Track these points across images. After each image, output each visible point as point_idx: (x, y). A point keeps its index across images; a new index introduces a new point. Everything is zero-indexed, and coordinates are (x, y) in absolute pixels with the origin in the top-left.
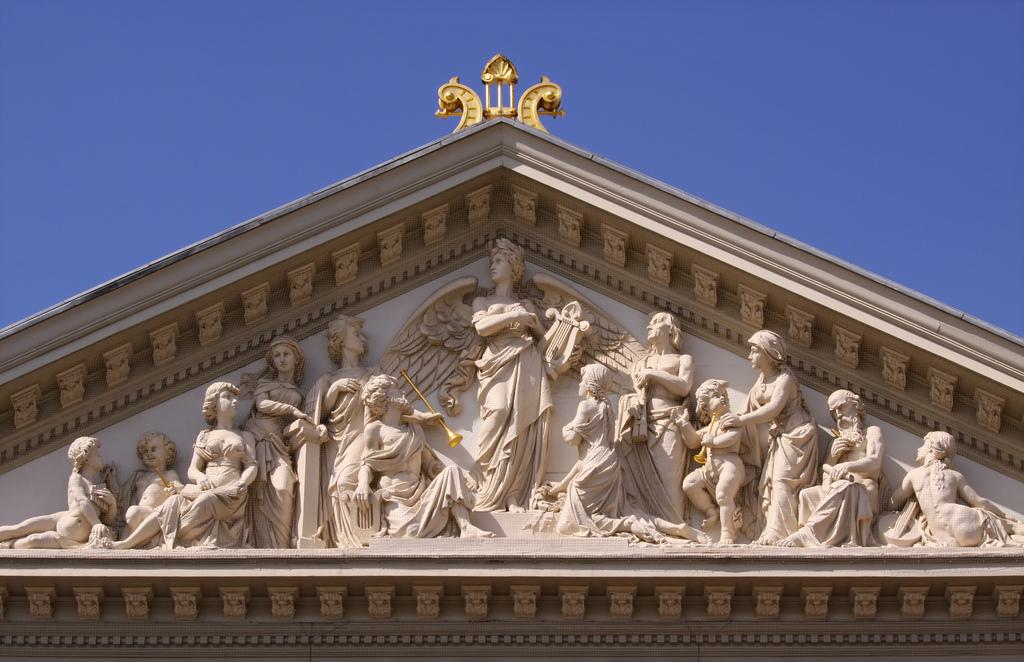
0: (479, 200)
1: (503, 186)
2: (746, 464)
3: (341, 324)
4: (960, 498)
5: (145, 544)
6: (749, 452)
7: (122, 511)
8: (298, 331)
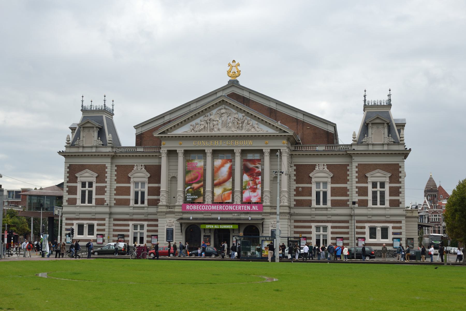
4: (258, 128)
5: (196, 132)
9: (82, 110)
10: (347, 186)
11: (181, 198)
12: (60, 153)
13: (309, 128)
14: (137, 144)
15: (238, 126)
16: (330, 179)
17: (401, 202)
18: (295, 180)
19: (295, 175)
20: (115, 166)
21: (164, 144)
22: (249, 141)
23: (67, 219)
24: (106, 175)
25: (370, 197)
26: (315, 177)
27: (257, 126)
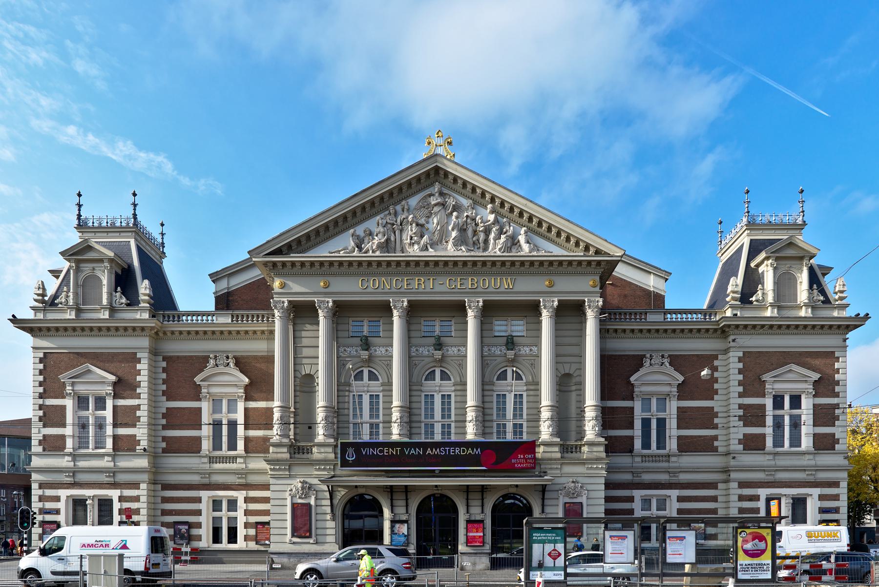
0: (432, 173)
1: (437, 169)
2: (486, 235)
3: (404, 202)
6: (487, 231)
7: (361, 245)
8: (395, 204)
10: (715, 404)
14: (217, 308)
16: (676, 389)
17: (838, 440)
20: (161, 358)
23: (42, 486)
24: (139, 378)
25: (769, 430)
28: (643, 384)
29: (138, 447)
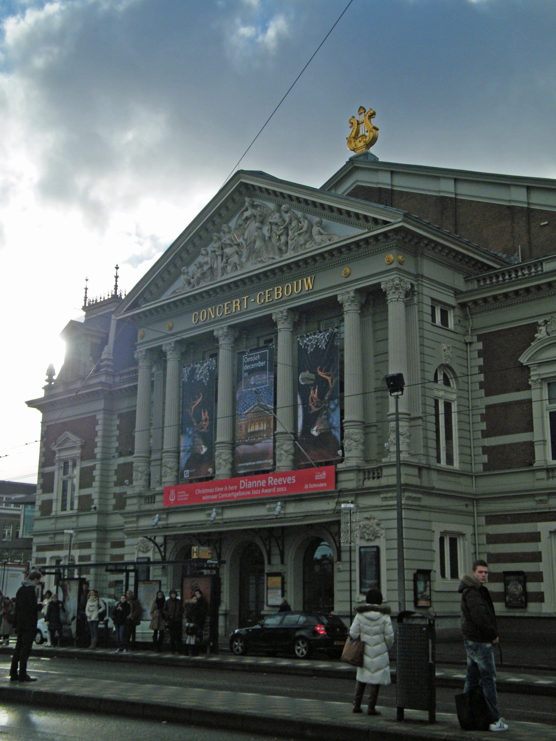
4: (321, 234)
5: (194, 286)
9: (84, 308)
11: (169, 471)
12: (31, 404)
13: (546, 223)
15: (278, 244)
18: (482, 385)
19: (480, 367)
20: (116, 417)
21: (142, 338)
22: (305, 280)
26: (540, 364)
27: (318, 228)
28: (540, 363)
29: (93, 506)
